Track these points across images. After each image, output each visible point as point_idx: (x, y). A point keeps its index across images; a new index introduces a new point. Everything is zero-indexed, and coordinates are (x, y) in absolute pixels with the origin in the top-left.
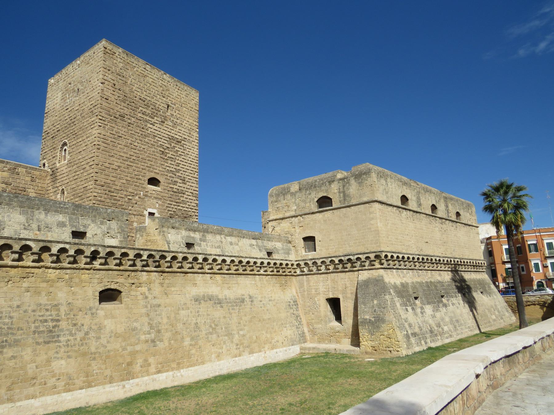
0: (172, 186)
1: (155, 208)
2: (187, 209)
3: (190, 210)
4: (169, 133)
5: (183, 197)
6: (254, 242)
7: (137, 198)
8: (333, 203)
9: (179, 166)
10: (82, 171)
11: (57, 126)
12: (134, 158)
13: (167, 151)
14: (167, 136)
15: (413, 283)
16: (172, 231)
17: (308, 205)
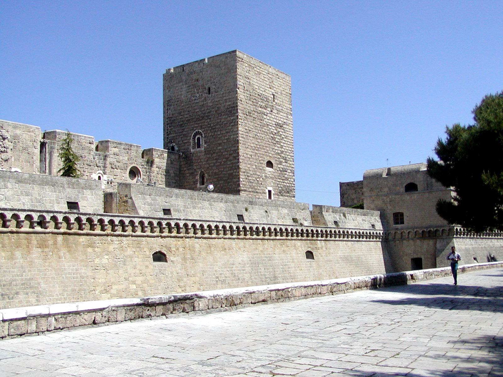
0: (279, 166)
1: (272, 186)
2: (288, 185)
3: (290, 185)
4: (275, 120)
5: (286, 174)
6: (363, 217)
7: (261, 179)
8: (418, 187)
9: (282, 148)
11: (186, 116)
12: (258, 146)
13: (275, 136)
14: (274, 123)
15: (473, 248)
16: (327, 214)
17: (398, 188)
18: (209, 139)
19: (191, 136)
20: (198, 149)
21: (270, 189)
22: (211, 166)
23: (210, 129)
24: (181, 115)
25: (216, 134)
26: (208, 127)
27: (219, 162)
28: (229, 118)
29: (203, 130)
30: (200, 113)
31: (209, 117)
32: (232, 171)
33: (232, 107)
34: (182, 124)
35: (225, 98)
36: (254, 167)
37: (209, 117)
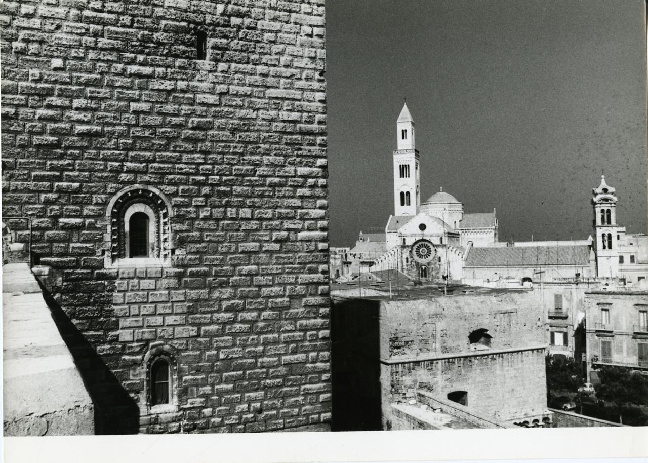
18: (201, 230)
19: (105, 203)
20: (139, 263)
22: (210, 335)
23: (206, 190)
24: (49, 107)
26: (196, 183)
27: (243, 321)
28: (290, 169)
29: (171, 189)
32: (301, 356)
33: (302, 133)
34: (52, 146)
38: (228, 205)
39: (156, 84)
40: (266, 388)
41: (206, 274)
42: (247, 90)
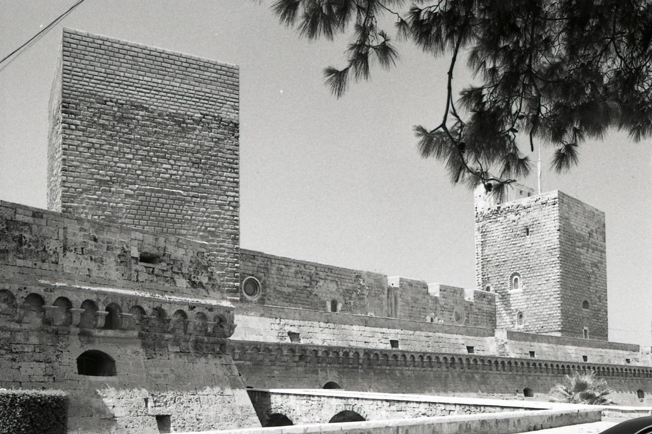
10: (544, 301)
11: (502, 257)
21: (586, 328)
25: (535, 274)
30: (518, 254)
31: (528, 258)
33: (552, 249)
35: (544, 240)
36: (573, 307)
37: (528, 258)
38: (534, 273)
39: (518, 245)
40: (544, 321)
41: (529, 292)
42: (538, 241)
